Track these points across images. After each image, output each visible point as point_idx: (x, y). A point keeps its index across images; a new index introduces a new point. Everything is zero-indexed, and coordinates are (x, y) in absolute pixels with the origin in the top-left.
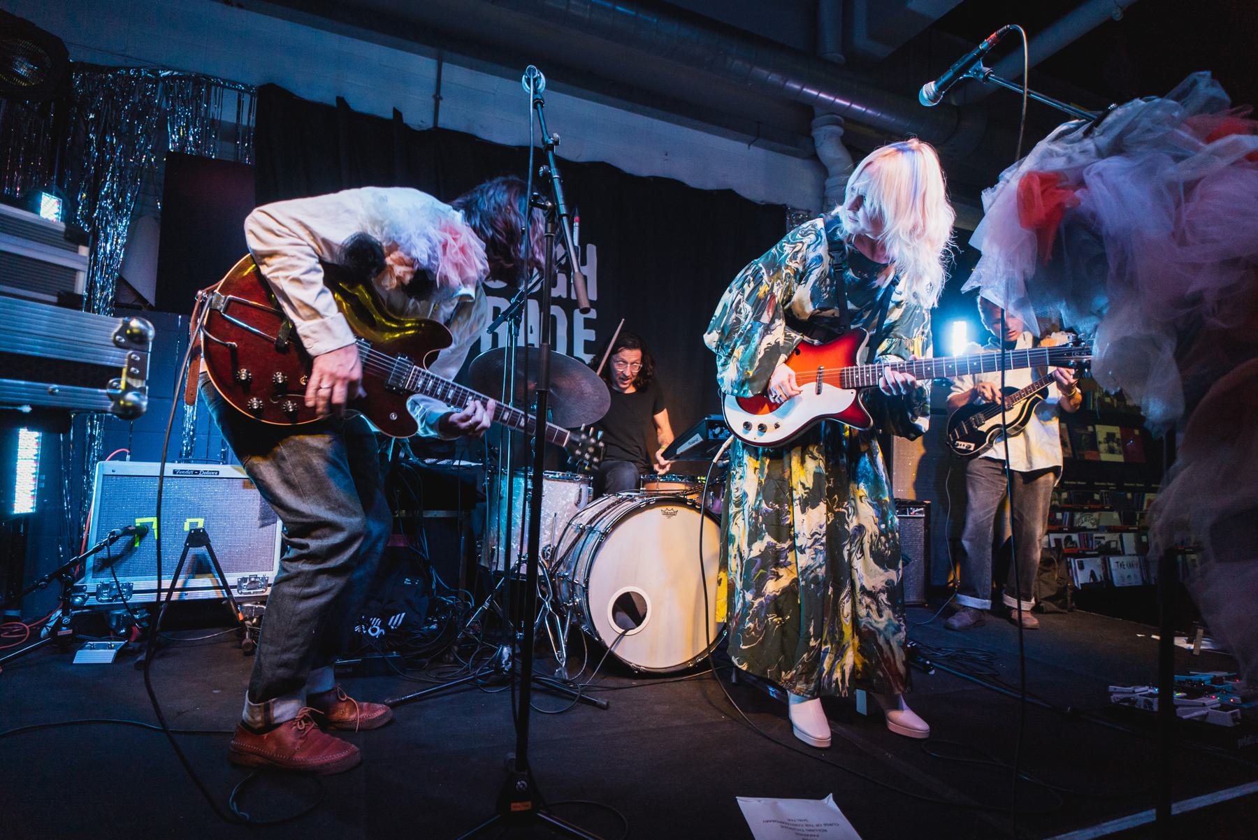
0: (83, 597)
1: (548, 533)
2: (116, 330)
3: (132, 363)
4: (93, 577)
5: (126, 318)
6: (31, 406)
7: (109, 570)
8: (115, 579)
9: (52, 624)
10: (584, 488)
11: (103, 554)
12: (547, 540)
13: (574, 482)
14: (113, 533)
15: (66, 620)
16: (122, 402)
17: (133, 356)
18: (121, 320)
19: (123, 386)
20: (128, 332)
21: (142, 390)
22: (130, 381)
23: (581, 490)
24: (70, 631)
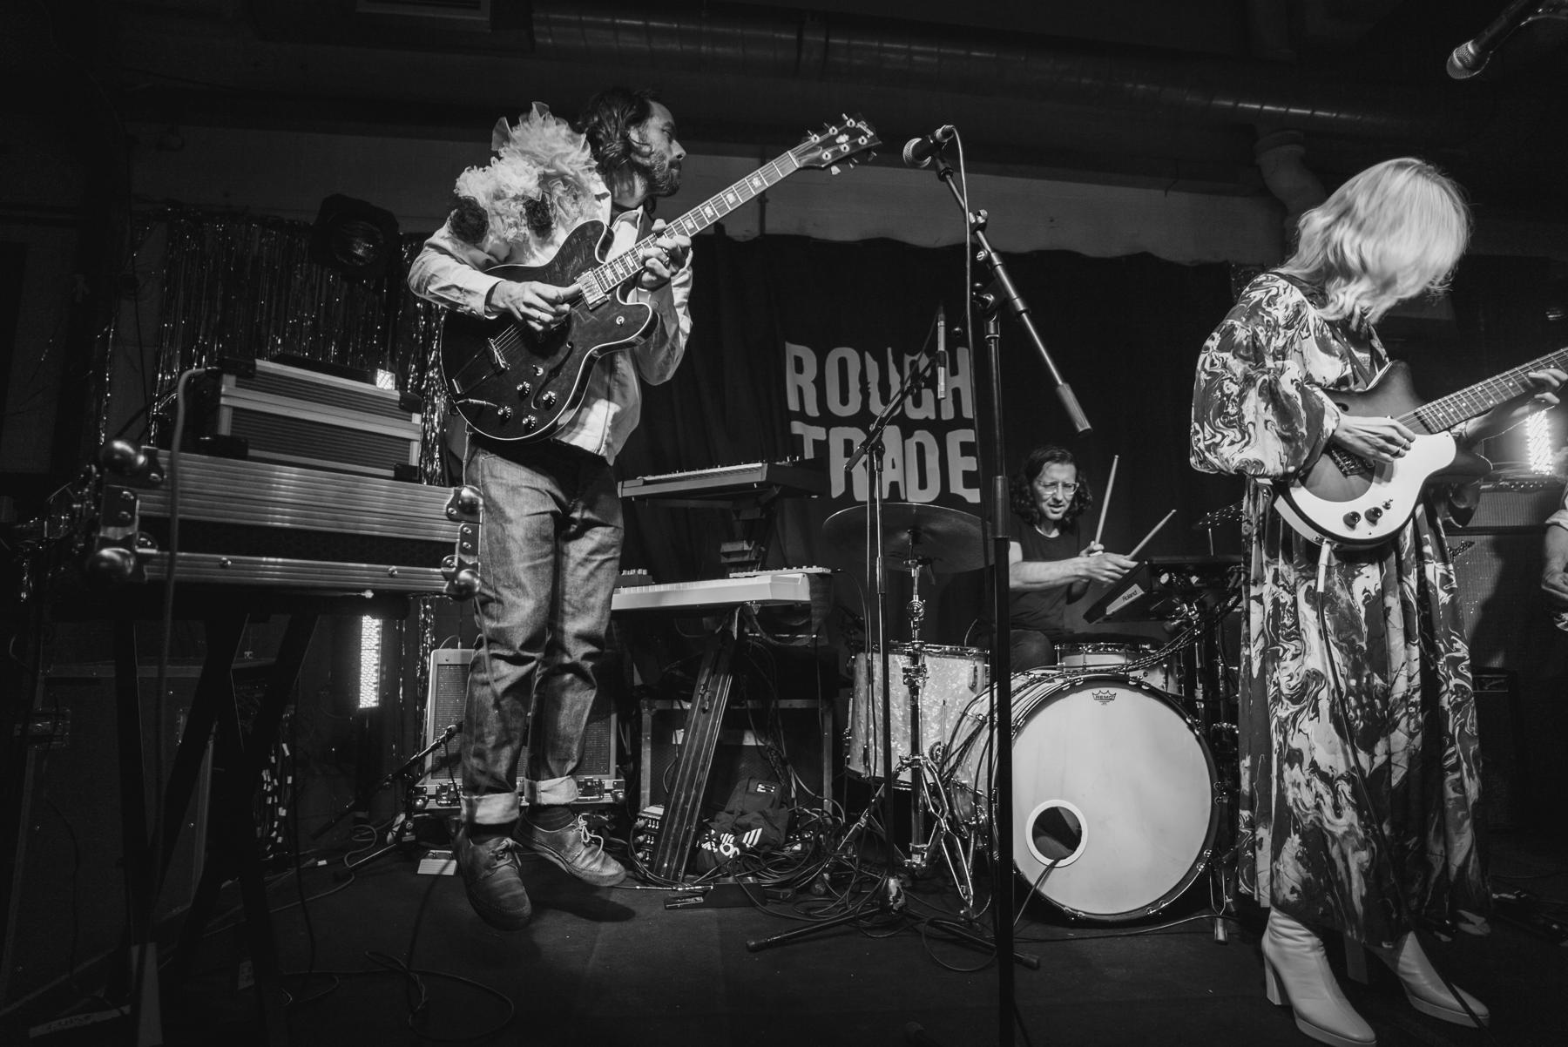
0: (423, 799)
1: (936, 726)
2: (448, 502)
3: (464, 536)
4: (432, 778)
5: (457, 488)
6: (373, 591)
7: (447, 771)
8: (453, 781)
9: (396, 829)
10: (980, 665)
11: (441, 752)
12: (935, 737)
13: (966, 659)
14: (450, 730)
15: (409, 824)
16: (456, 582)
17: (465, 529)
18: (453, 489)
19: (456, 563)
20: (460, 502)
21: (475, 566)
22: (463, 557)
23: (976, 668)
24: (413, 838)
